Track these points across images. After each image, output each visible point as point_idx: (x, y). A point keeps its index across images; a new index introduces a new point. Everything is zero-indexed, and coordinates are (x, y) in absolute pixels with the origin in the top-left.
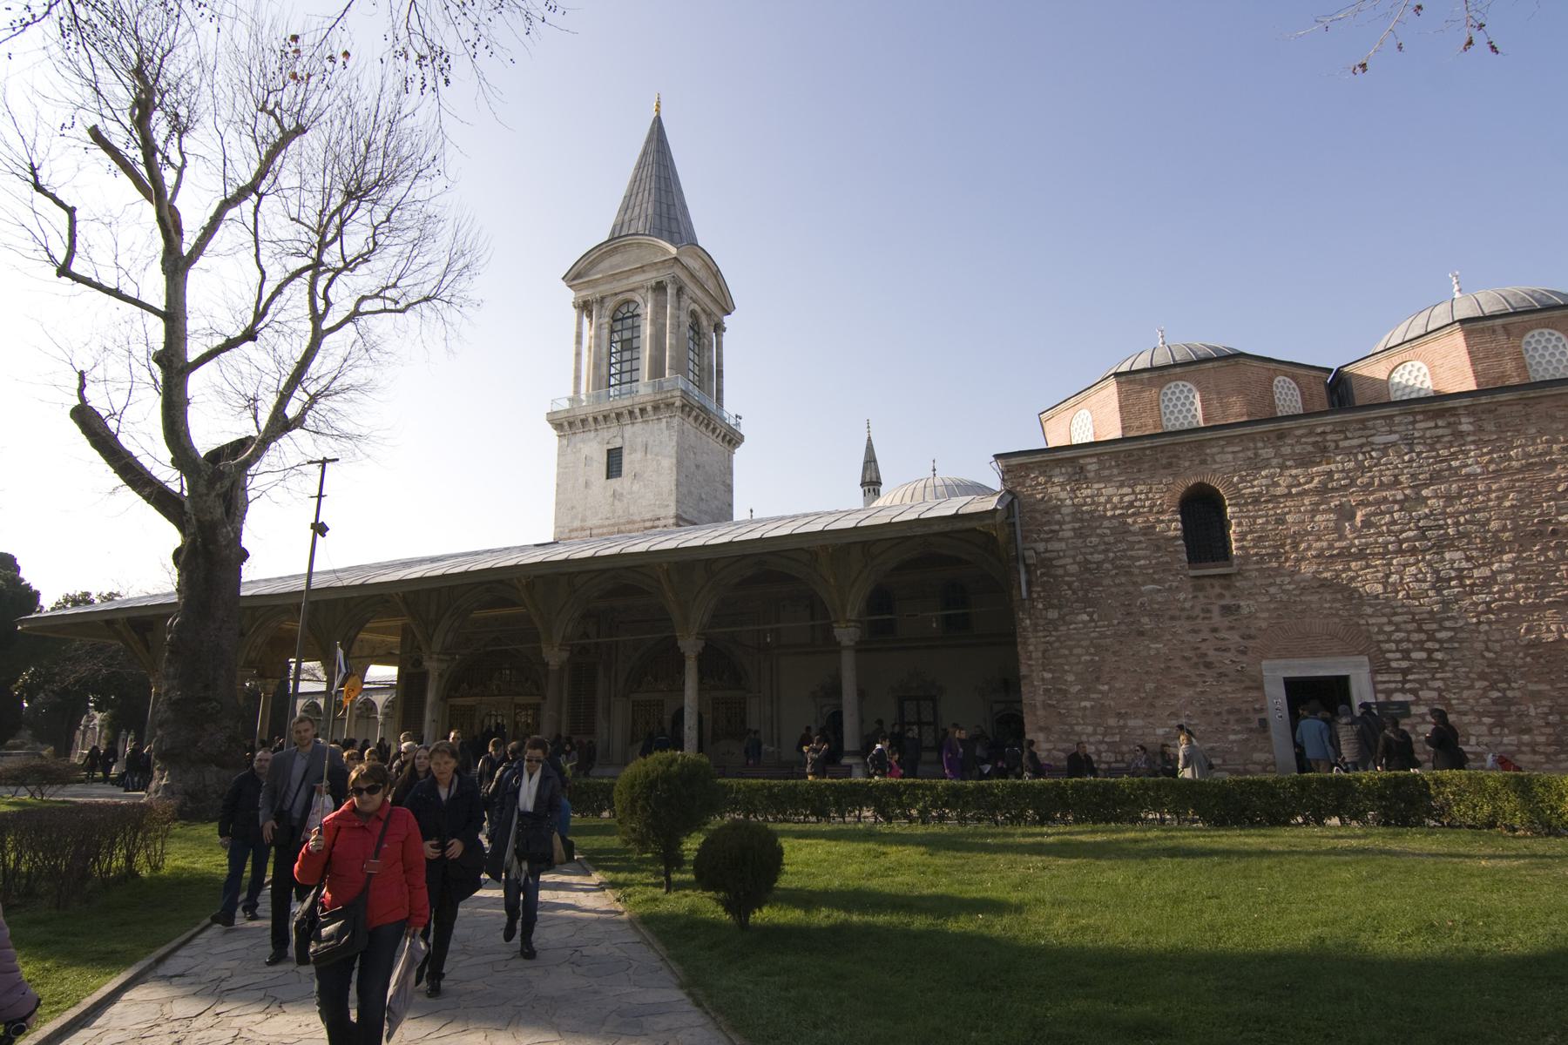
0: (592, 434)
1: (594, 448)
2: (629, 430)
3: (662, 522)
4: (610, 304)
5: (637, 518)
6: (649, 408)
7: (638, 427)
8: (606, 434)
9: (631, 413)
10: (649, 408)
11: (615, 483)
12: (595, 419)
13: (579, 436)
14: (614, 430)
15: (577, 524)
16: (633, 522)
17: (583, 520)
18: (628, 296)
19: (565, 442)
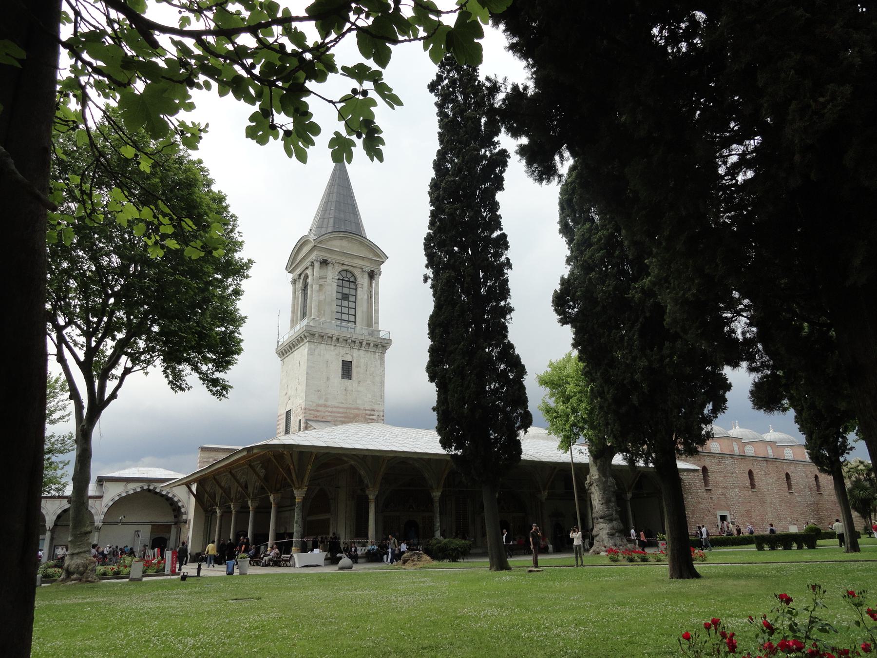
0: (332, 348)
1: (333, 356)
2: (356, 353)
3: (376, 413)
4: (339, 268)
5: (360, 407)
6: (372, 344)
7: (362, 353)
8: (342, 351)
9: (361, 343)
10: (372, 344)
11: (346, 381)
12: (338, 339)
13: (323, 346)
14: (348, 350)
15: (322, 402)
16: (358, 409)
17: (326, 400)
18: (350, 269)
19: (313, 346)
